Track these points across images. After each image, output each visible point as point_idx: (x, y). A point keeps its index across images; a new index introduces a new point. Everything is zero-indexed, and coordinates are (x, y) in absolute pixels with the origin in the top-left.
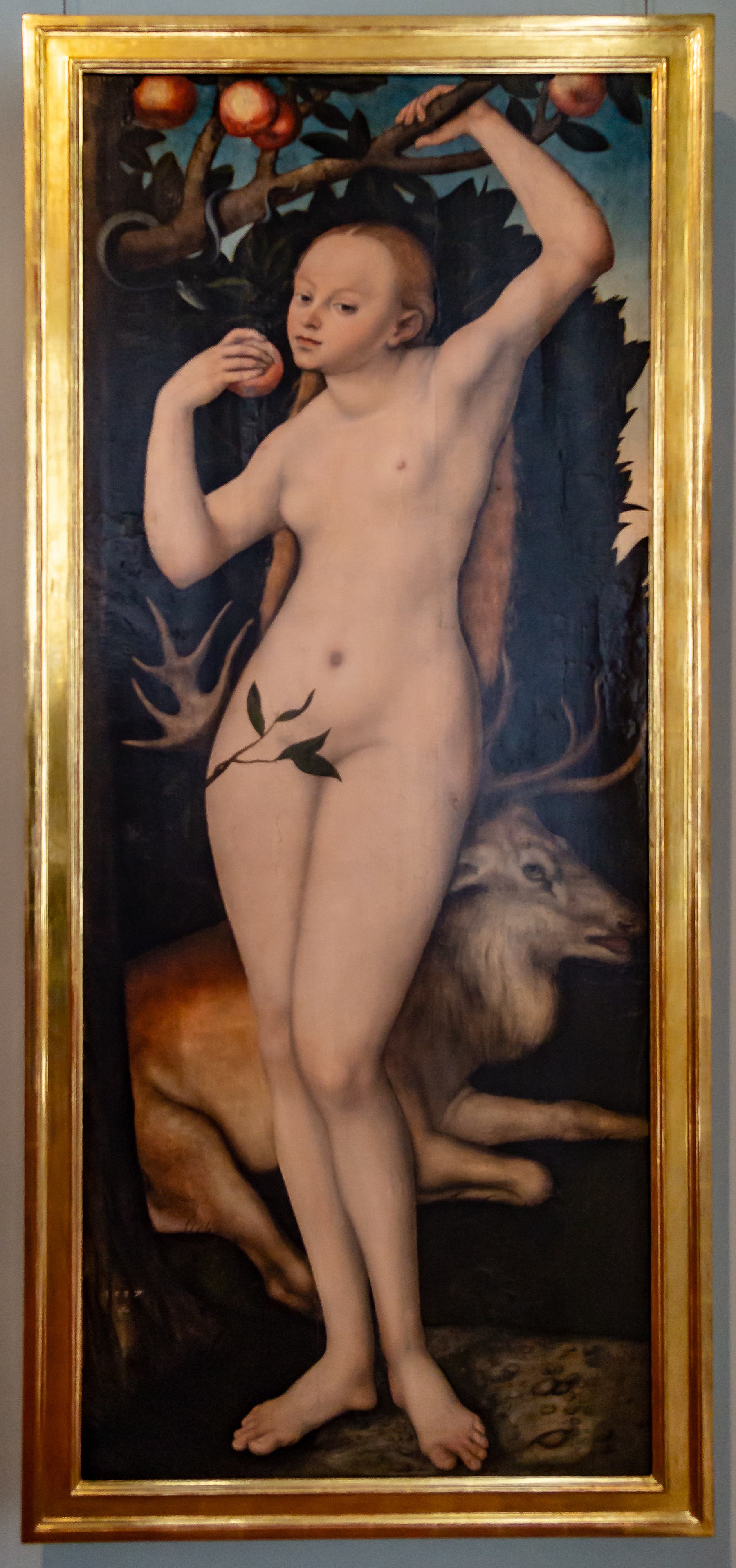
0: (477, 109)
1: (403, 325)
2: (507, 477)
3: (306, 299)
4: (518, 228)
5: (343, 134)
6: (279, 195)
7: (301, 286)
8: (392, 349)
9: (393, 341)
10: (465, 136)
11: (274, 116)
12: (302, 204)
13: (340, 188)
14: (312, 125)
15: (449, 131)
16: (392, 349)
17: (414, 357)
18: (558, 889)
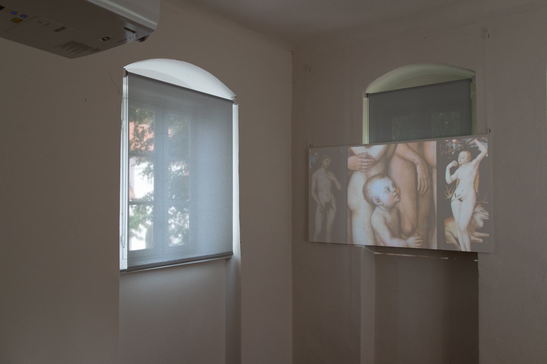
0: (475, 139)
1: (468, 160)
2: (478, 173)
3: (460, 158)
4: (479, 150)
5: (463, 142)
6: (457, 148)
7: (459, 156)
8: (467, 162)
9: (468, 161)
10: (474, 142)
11: (457, 141)
12: (459, 149)
13: (463, 147)
14: (460, 142)
15: (473, 142)
16: (467, 162)
17: (469, 163)
18: (483, 212)
